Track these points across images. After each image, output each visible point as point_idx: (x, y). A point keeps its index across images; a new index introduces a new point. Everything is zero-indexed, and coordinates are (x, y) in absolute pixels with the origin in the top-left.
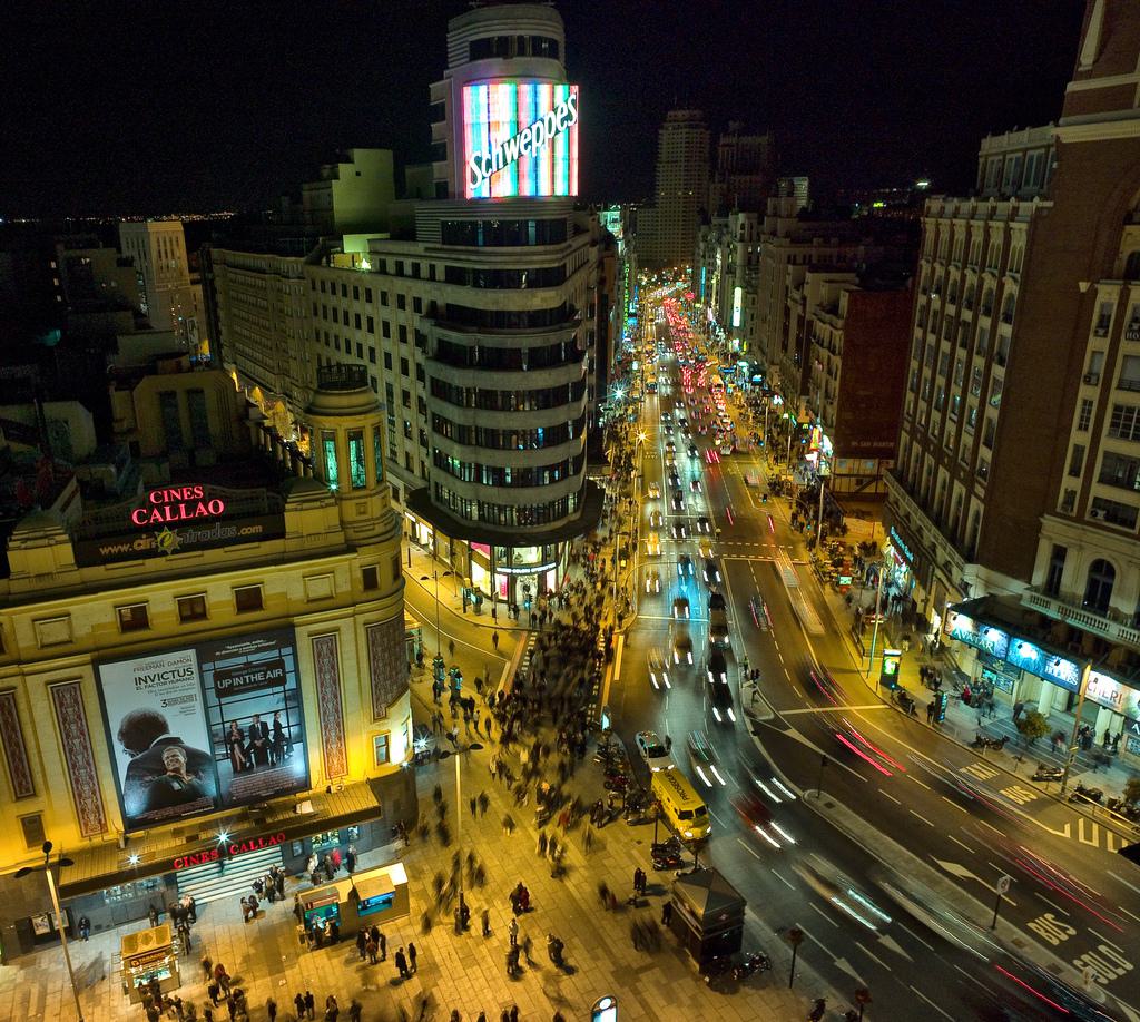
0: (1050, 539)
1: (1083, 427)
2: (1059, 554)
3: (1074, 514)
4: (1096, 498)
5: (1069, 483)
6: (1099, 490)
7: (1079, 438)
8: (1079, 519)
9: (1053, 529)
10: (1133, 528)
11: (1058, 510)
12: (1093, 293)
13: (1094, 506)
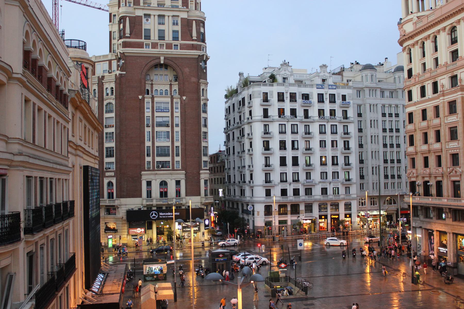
0: (145, 180)
2: (149, 184)
3: (151, 169)
5: (148, 159)
6: (158, 159)
7: (148, 144)
8: (154, 170)
9: (146, 176)
10: (170, 168)
11: (146, 169)
12: (144, 98)
13: (157, 164)
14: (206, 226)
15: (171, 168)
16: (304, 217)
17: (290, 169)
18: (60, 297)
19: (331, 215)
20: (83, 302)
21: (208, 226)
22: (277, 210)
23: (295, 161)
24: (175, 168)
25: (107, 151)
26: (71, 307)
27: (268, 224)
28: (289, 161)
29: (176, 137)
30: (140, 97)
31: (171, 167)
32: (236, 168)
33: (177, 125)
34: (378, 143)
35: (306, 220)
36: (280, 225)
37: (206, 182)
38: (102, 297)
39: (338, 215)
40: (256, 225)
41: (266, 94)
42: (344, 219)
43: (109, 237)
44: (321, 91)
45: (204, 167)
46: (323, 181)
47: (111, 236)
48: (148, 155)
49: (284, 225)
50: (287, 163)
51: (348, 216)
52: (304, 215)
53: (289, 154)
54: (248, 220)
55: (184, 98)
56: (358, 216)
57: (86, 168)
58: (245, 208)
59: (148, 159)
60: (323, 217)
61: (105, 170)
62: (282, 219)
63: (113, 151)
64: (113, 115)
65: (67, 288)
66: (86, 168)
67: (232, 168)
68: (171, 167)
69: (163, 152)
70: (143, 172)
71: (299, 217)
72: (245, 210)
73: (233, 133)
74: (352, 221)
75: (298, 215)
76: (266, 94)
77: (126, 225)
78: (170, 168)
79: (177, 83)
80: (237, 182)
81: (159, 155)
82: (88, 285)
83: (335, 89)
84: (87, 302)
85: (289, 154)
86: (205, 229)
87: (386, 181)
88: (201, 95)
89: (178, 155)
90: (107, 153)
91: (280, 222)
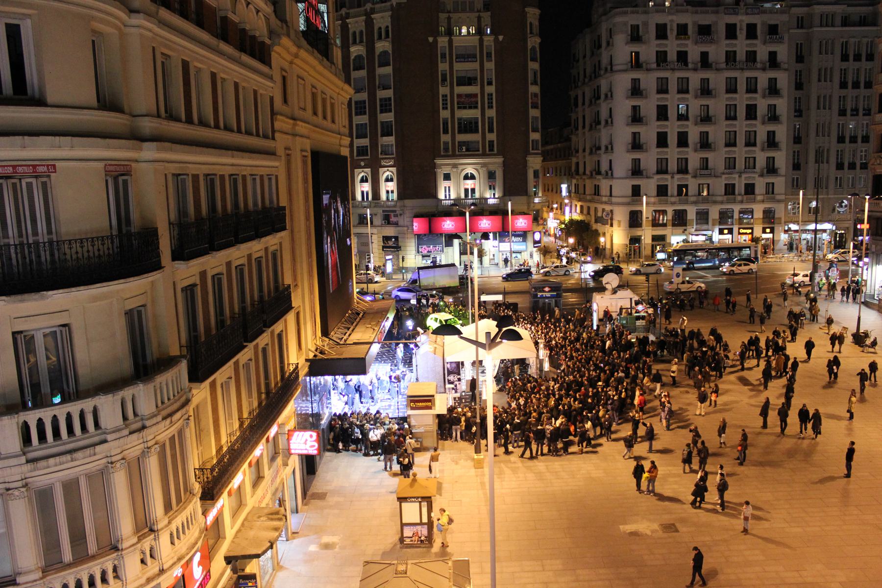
1: (445, 108)
3: (450, 153)
4: (459, 142)
5: (445, 138)
10: (479, 151)
11: (442, 153)
13: (459, 146)
14: (535, 242)
15: (481, 152)
16: (694, 230)
17: (673, 153)
18: (264, 350)
19: (739, 229)
20: (315, 356)
21: (539, 242)
22: (650, 219)
23: (683, 140)
24: (487, 152)
25: (382, 127)
26: (291, 362)
27: (635, 240)
28: (672, 139)
29: (489, 103)
30: (431, 39)
31: (481, 149)
32: (588, 151)
33: (490, 83)
34: (830, 109)
35: (697, 235)
36: (654, 243)
37: (536, 174)
38: (344, 349)
39: (752, 229)
40: (614, 242)
41: (635, 29)
42: (758, 236)
43: (388, 257)
44: (731, 19)
45: (533, 149)
46: (728, 171)
47: (390, 257)
48: (446, 131)
49: (660, 243)
50: (669, 142)
51: (768, 230)
52: (695, 227)
53: (672, 128)
54: (604, 234)
55: (501, 38)
56: (786, 232)
57: (316, 156)
58: (599, 214)
59: (445, 138)
60: (726, 231)
61: (380, 156)
62: (659, 232)
63: (392, 126)
64: (388, 70)
65: (280, 336)
66: (316, 156)
67: (581, 151)
68: (481, 149)
69: (469, 127)
70: (438, 161)
71: (685, 230)
72: (599, 217)
73: (584, 93)
74: (775, 239)
75: (684, 228)
76: (635, 29)
77: (414, 241)
78: (479, 151)
79: (489, 13)
80: (588, 172)
81: (460, 132)
82: (325, 333)
83: (758, 14)
84: (320, 356)
85: (672, 128)
86: (534, 247)
87: (839, 174)
88: (529, 32)
89: (491, 130)
90: (382, 131)
91: (655, 238)
